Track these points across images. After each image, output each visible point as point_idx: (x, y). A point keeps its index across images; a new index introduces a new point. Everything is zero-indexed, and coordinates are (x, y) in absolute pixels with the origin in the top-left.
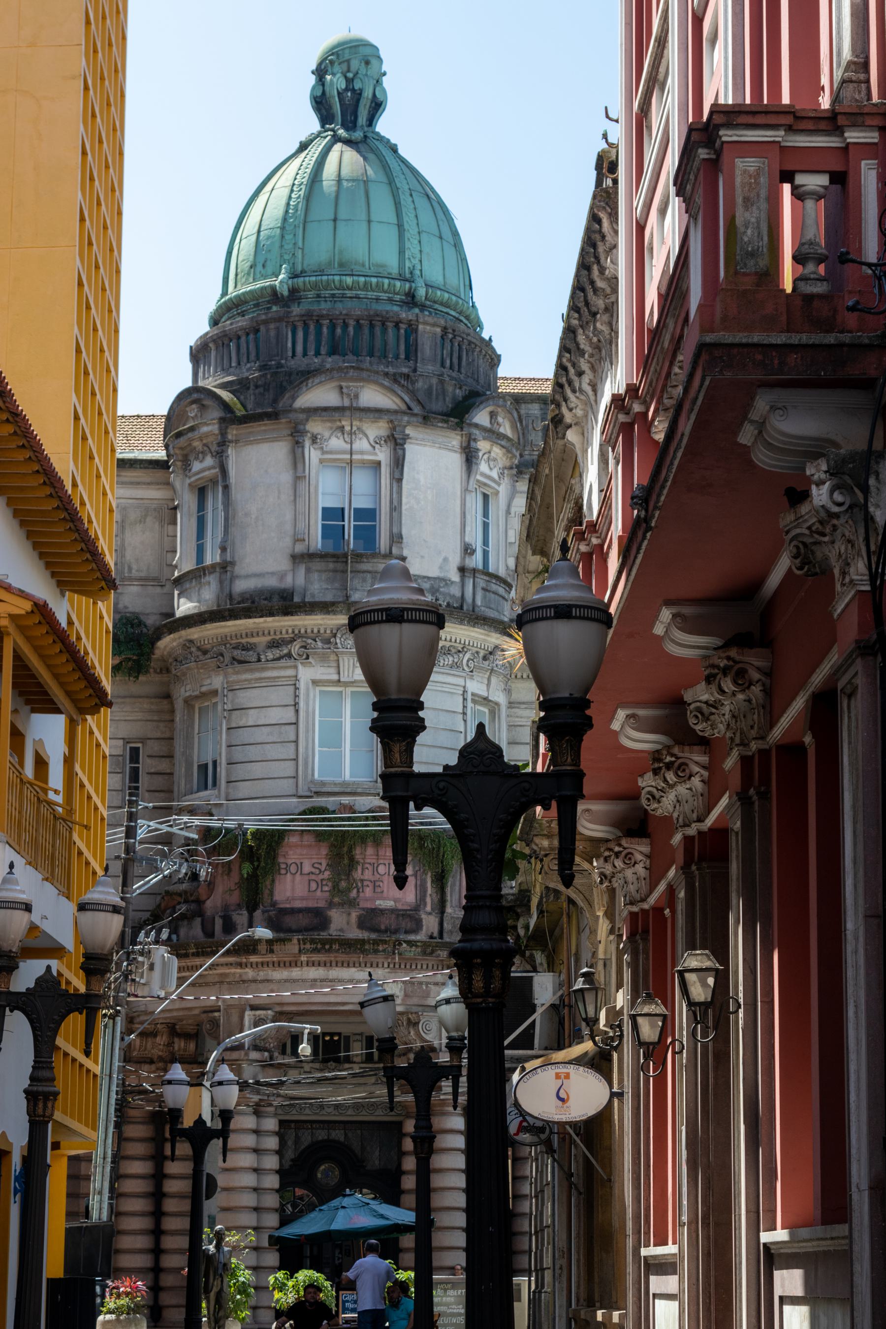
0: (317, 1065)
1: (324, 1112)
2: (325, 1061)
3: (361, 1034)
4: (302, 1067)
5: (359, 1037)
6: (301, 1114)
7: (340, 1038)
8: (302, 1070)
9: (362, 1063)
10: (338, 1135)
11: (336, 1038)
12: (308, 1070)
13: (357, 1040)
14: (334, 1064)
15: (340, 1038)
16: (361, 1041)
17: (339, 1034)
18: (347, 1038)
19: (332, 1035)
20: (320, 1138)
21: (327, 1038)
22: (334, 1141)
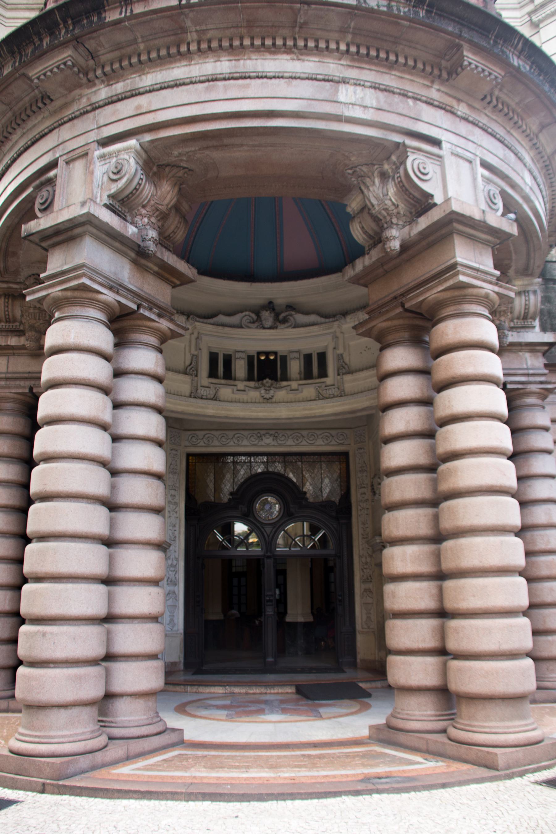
0: (252, 384)
1: (262, 443)
2: (261, 378)
3: (298, 352)
4: (235, 385)
5: (296, 355)
6: (238, 445)
7: (276, 357)
8: (235, 388)
9: (301, 379)
10: (278, 467)
11: (272, 358)
12: (242, 388)
13: (295, 358)
14: (270, 381)
15: (276, 357)
16: (299, 359)
17: (275, 353)
18: (284, 359)
19: (267, 354)
20: (259, 471)
21: (263, 358)
22: (273, 473)
